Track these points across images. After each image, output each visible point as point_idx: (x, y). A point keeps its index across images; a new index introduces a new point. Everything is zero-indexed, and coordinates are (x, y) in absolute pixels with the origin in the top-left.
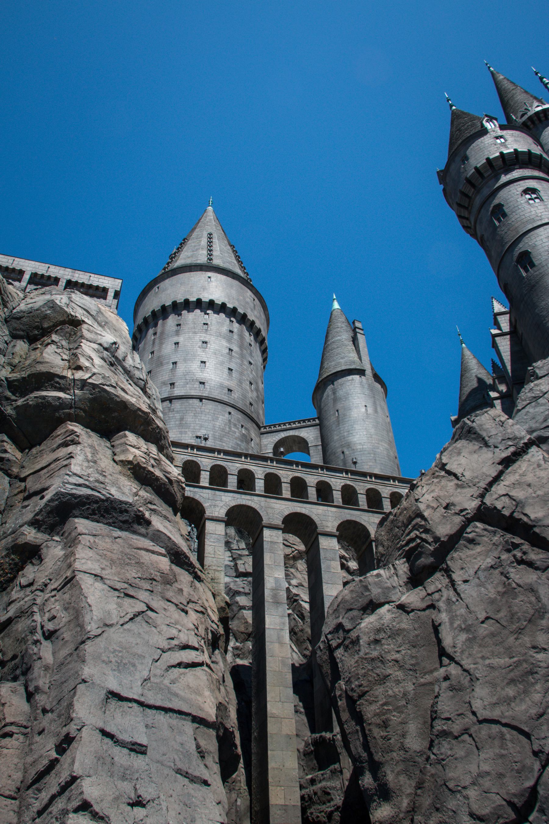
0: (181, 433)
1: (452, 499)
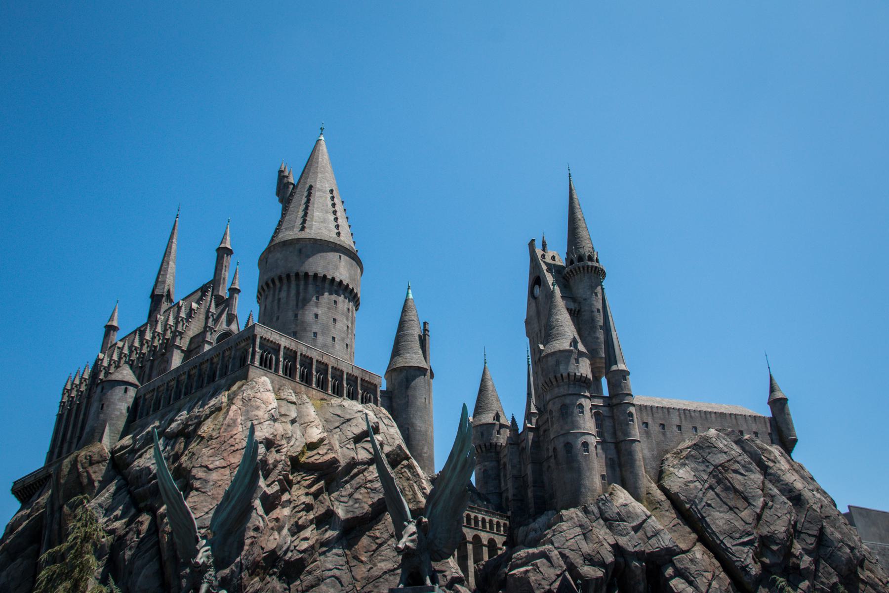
1: (541, 582)
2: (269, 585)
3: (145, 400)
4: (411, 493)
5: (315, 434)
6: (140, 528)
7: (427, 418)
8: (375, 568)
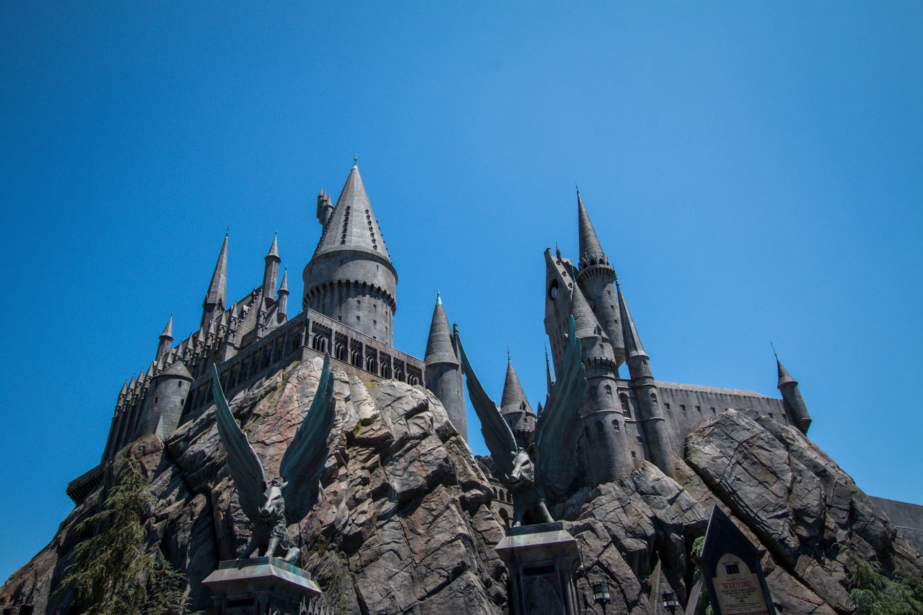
1: (589, 554)
2: (329, 560)
3: (199, 392)
4: (462, 466)
5: (368, 411)
6: (194, 510)
7: (460, 408)
8: (432, 540)
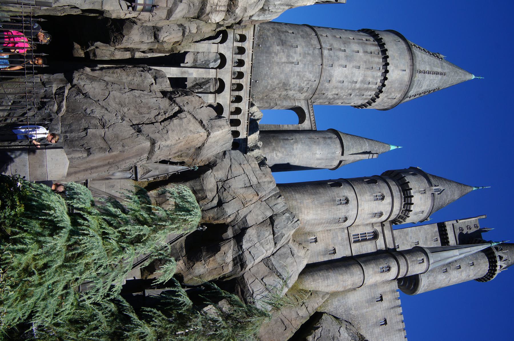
0: (300, 54)
